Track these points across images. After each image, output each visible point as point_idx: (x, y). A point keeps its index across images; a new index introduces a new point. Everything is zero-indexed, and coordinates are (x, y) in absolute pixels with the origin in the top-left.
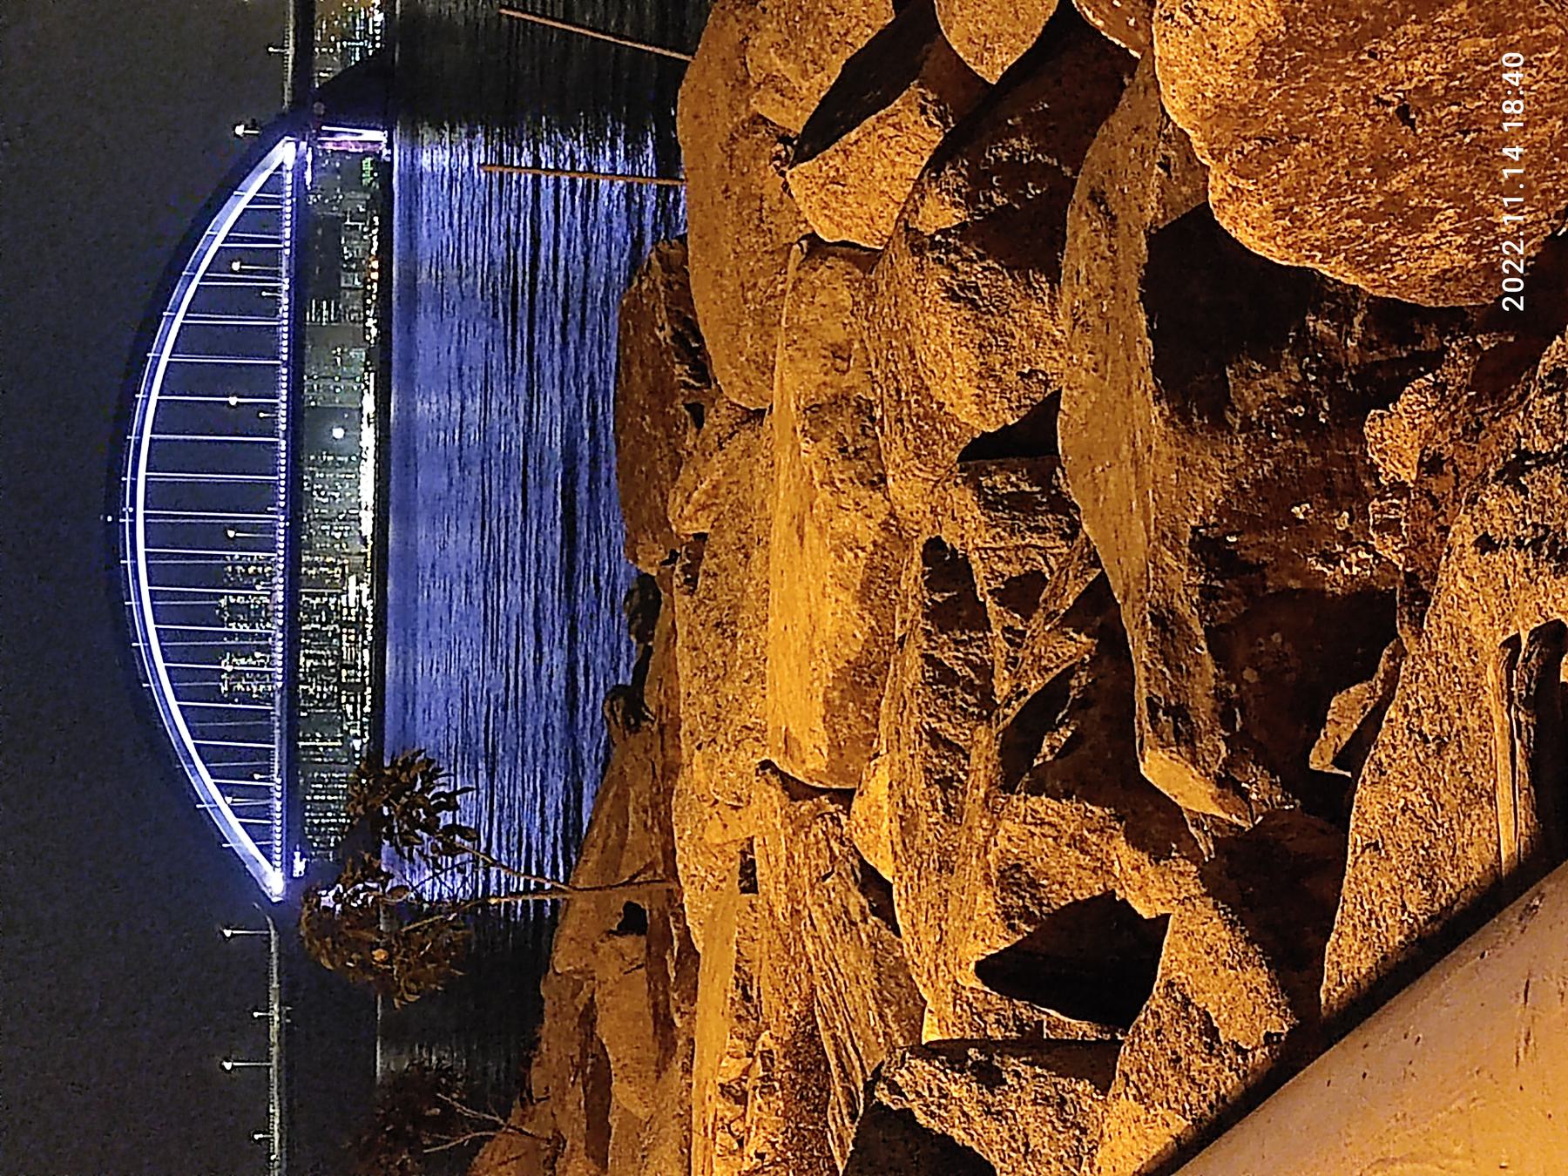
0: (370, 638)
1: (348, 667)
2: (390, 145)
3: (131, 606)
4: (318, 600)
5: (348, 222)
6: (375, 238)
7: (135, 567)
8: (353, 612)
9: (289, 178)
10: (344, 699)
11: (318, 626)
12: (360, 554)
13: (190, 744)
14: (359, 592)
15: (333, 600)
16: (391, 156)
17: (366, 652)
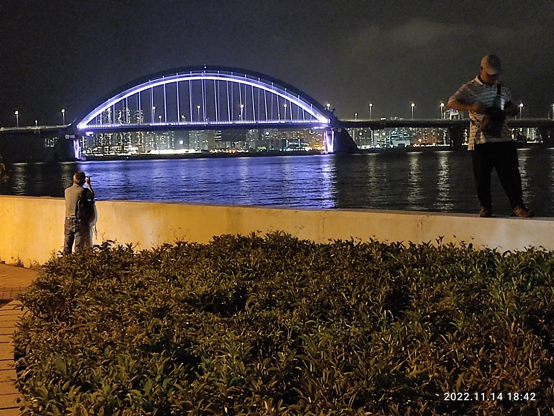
0: (119, 155)
1: (109, 149)
2: (329, 153)
3: (176, 75)
4: (130, 138)
5: (245, 143)
6: (241, 151)
7: (189, 76)
8: (127, 149)
9: (316, 121)
10: (99, 147)
11: (122, 138)
12: (145, 150)
13: (126, 96)
14: (133, 151)
15: (130, 143)
16: (324, 154)
17: (114, 154)
